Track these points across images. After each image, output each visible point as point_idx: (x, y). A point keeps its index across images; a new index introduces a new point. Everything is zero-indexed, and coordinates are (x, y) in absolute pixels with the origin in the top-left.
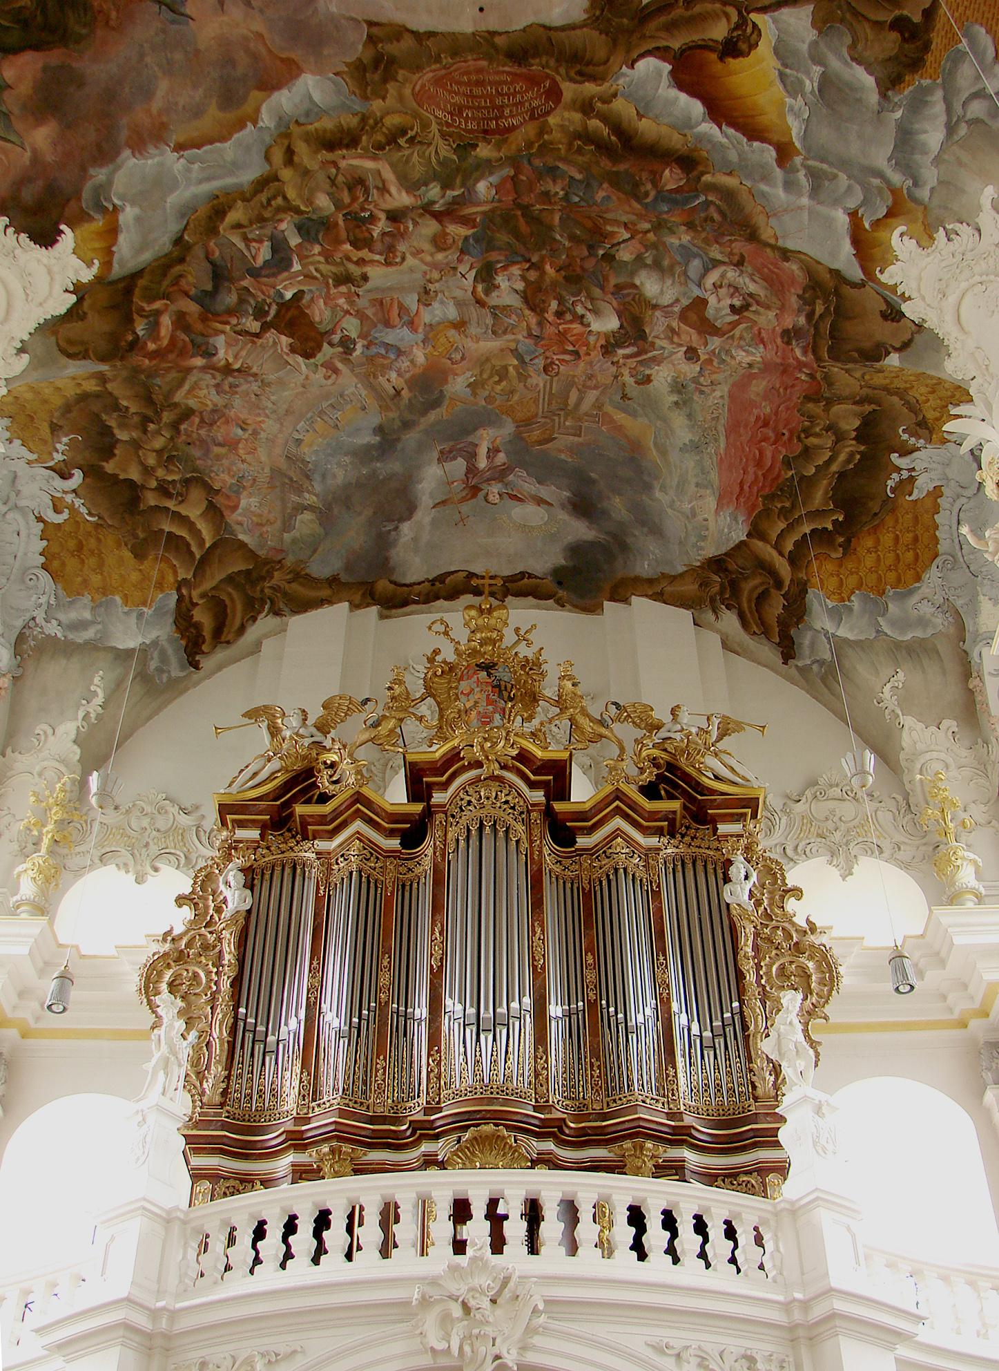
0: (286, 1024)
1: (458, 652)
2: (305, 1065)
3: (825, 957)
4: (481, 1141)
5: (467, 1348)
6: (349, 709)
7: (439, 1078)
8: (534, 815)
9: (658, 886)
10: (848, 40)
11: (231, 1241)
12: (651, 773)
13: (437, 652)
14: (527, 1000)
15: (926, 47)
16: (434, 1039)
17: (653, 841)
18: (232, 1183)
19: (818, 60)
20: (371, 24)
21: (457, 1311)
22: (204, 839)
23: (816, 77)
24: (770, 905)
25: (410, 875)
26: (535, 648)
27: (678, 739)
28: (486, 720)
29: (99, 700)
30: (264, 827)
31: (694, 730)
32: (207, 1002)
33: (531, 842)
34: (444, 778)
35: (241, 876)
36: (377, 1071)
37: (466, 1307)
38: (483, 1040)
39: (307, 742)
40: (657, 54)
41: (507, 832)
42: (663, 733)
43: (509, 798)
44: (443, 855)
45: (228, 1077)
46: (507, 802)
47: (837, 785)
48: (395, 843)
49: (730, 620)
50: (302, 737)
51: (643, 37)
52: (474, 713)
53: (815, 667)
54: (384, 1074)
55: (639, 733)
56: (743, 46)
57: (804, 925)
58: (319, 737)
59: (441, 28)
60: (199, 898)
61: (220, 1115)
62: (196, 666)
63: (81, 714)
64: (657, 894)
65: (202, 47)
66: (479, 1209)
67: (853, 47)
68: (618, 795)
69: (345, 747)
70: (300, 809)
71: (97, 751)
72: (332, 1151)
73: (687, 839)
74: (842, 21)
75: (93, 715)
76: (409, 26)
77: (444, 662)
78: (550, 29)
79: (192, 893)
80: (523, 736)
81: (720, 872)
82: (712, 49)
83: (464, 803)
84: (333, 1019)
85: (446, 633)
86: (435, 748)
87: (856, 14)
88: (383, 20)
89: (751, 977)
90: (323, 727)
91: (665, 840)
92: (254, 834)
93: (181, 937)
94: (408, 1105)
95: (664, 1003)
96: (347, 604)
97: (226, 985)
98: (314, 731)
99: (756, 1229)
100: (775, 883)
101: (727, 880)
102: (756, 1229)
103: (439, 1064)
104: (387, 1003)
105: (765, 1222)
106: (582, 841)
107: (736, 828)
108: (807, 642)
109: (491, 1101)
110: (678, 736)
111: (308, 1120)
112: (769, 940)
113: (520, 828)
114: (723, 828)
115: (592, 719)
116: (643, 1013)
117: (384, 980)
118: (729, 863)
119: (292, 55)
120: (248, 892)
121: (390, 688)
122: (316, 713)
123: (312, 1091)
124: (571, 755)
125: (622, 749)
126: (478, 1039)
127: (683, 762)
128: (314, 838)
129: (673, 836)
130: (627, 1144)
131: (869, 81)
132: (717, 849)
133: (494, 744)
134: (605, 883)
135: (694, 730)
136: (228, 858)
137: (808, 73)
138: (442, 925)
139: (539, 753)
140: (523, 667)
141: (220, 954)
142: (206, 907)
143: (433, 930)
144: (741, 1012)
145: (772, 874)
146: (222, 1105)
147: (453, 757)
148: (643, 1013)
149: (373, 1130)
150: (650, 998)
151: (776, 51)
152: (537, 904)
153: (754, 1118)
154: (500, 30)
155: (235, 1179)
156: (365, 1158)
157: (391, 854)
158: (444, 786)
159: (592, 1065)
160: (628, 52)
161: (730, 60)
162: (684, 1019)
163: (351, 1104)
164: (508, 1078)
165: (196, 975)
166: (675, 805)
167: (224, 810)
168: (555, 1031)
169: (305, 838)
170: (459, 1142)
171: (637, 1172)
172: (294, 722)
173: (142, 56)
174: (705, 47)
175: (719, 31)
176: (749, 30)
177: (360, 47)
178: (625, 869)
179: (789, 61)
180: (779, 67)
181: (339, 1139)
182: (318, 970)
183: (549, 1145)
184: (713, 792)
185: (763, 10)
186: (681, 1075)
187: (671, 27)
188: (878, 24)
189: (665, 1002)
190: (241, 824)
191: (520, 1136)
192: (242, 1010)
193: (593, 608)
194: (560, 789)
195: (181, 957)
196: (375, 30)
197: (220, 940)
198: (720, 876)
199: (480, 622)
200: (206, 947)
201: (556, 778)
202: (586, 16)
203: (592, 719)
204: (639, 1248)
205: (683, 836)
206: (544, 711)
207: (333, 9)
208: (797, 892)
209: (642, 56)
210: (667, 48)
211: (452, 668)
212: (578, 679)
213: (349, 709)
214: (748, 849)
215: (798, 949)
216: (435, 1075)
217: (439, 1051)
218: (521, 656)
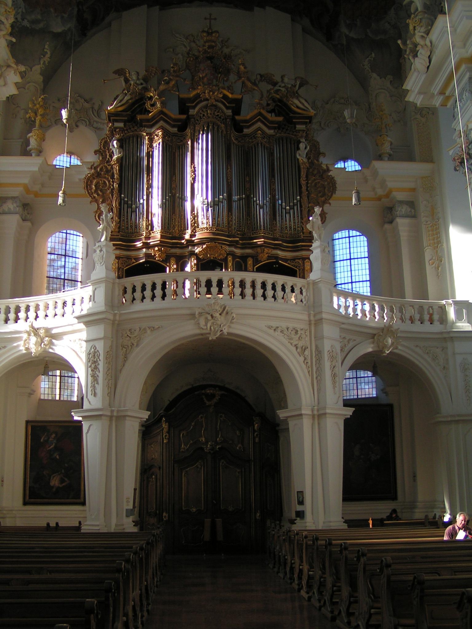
0: (139, 201)
5: (212, 328)
6: (156, 72)
8: (228, 120)
11: (134, 290)
14: (225, 194)
17: (271, 132)
18: (124, 259)
21: (210, 318)
25: (181, 143)
29: (48, 55)
30: (125, 122)
31: (290, 86)
32: (110, 193)
33: (227, 131)
34: (194, 104)
37: (212, 316)
39: (140, 87)
41: (218, 128)
42: (277, 88)
45: (120, 222)
46: (218, 115)
48: (175, 130)
50: (138, 84)
52: (206, 79)
57: (325, 168)
60: (103, 151)
61: (118, 236)
62: (85, 35)
63: (42, 63)
66: (214, 284)
68: (260, 114)
70: (139, 117)
71: (50, 76)
73: (284, 130)
75: (46, 62)
77: (194, 55)
80: (224, 88)
81: (296, 144)
83: (202, 115)
91: (276, 131)
92: (121, 125)
93: (97, 167)
96: (146, 6)
97: (116, 185)
98: (142, 81)
99: (301, 288)
101: (298, 149)
102: (301, 288)
104: (175, 195)
105: (304, 286)
106: (246, 131)
107: (303, 127)
110: (283, 89)
113: (223, 125)
114: (298, 127)
118: (299, 142)
120: (121, 150)
121: (173, 67)
122: (143, 73)
125: (262, 95)
127: (284, 100)
128: (145, 127)
129: (279, 129)
132: (295, 135)
134: (253, 149)
135: (290, 86)
136: (112, 135)
139: (230, 96)
140: (225, 58)
141: (113, 174)
142: (106, 155)
144: (300, 201)
146: (119, 232)
147: (198, 96)
149: (173, 243)
152: (229, 158)
153: (303, 241)
157: (174, 135)
158: (194, 107)
162: (280, 201)
165: (105, 182)
166: (280, 119)
168: (234, 205)
169: (142, 126)
172: (134, 77)
181: (160, 245)
183: (233, 249)
184: (295, 113)
186: (278, 223)
189: (273, 196)
190: (117, 121)
192: (123, 195)
193: (251, 9)
194: (237, 111)
197: (112, 168)
198: (296, 146)
199: (208, 38)
200: (107, 171)
203: (251, 82)
204: (264, 296)
205: (283, 128)
206: (233, 77)
211: (197, 58)
213: (156, 72)
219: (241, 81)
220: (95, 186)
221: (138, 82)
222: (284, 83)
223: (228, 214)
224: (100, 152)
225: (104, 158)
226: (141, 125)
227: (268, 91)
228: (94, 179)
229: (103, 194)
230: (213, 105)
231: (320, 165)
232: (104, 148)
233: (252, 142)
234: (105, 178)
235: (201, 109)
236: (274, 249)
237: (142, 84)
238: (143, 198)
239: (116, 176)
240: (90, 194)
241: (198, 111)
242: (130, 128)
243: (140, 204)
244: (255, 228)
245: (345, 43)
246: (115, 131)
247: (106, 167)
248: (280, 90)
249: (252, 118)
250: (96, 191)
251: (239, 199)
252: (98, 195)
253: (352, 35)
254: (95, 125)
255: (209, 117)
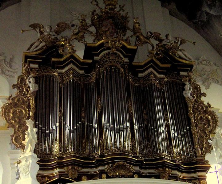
0: (52, 127)
1: (102, 12)
2: (60, 141)
3: (214, 115)
4: (119, 167)
7: (103, 146)
9: (164, 90)
12: (162, 55)
13: (95, 11)
16: (101, 134)
17: (161, 76)
22: (8, 65)
24: (196, 98)
26: (126, 12)
27: (169, 45)
28: (112, 35)
31: (173, 42)
33: (125, 74)
35: (34, 79)
36: (83, 143)
38: (118, 136)
39: (53, 37)
41: (119, 71)
43: (119, 60)
44: (99, 77)
46: (118, 61)
47: (205, 60)
48: (82, 72)
49: (174, 6)
50: (51, 35)
53: (199, 23)
54: (85, 144)
55: (158, 42)
58: (56, 36)
60: (20, 85)
64: (163, 93)
68: (152, 61)
69: (66, 40)
72: (72, 169)
77: (97, 14)
79: (18, 84)
80: (123, 40)
84: (68, 126)
85: (97, 5)
86: (95, 43)
89: (193, 120)
90: (57, 32)
92: (36, 66)
94: (93, 154)
95: (168, 127)
98: (54, 33)
100: (198, 91)
101: (184, 90)
103: (103, 142)
107: (185, 73)
108: (199, 14)
109: (121, 154)
110: (169, 44)
111: (63, 159)
112: (197, 109)
113: (122, 70)
115: (144, 36)
116: (163, 130)
117: (83, 115)
118: (184, 85)
120: (37, 85)
122: (55, 27)
123: (63, 148)
124: (137, 48)
125: (153, 47)
126: (115, 135)
130: (161, 169)
132: (180, 80)
133: (115, 43)
138: (100, 99)
139: (128, 47)
140: (122, 18)
141: (29, 105)
142: (23, 89)
143: (98, 101)
145: (196, 89)
147: (102, 45)
148: (163, 130)
150: (164, 126)
153: (196, 163)
155: (40, 176)
156: (81, 170)
157: (82, 75)
158: (98, 55)
159: (148, 144)
163: (76, 154)
164: (125, 147)
165: (22, 111)
166: (169, 66)
167: (27, 57)
168: (136, 133)
170: (112, 166)
171: (163, 178)
172: (48, 30)
178: (154, 84)
182: (61, 112)
183: (138, 168)
191: (131, 165)
194: (132, 59)
195: (16, 105)
197: (29, 100)
200: (24, 102)
201: (131, 54)
206: (129, 33)
208: (205, 95)
211: (99, 17)
212: (141, 23)
214: (190, 81)
215: (206, 112)
216: (102, 145)
217: (103, 138)
218: (121, 14)
219: (136, 35)
220: (13, 113)
221: (51, 33)
222: (169, 40)
223: (132, 138)
224: (18, 86)
225: (21, 91)
226: (55, 66)
227: (157, 45)
228: (12, 108)
229: (20, 120)
230: (114, 53)
231: (202, 102)
232: (21, 83)
233: (147, 83)
234: (22, 107)
235: (104, 56)
236: (174, 169)
237: (54, 35)
238: (55, 125)
239: (32, 106)
240: (8, 121)
241: (102, 57)
242: (44, 70)
243: (53, 130)
244: (154, 152)
245: (205, 19)
246: (31, 70)
247: (22, 99)
248: (166, 44)
249: (146, 64)
250: (13, 118)
251: (139, 128)
252: (15, 121)
253: (212, 12)
254: (7, 73)
255: (111, 62)
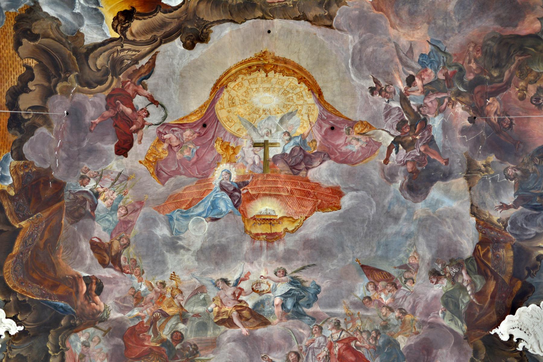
10: (62, 28)
15: (16, 27)
19: (78, 16)
20: (330, 27)
23: (77, 6)
40: (170, 9)
51: (178, 18)
56: (121, 18)
59: (291, 22)
65: (425, 24)
67: (59, 25)
74: (67, 38)
76: (309, 24)
78: (231, 21)
82: (140, 14)
87: (60, 41)
88: (323, 28)
119: (376, 12)
131: (46, 9)
137: (83, 7)
151: (102, 17)
154: (259, 20)
160: (187, 9)
161: (128, 9)
173: (460, 26)
174: (143, 15)
175: (136, 25)
176: (119, 28)
177: (337, 14)
179: (94, 12)
180: (99, 8)
185: (112, 40)
187: (163, 24)
188: (47, 36)
196: (328, 23)
202: (211, 28)
207: (350, 37)
209: (179, 7)
210: (165, 12)
